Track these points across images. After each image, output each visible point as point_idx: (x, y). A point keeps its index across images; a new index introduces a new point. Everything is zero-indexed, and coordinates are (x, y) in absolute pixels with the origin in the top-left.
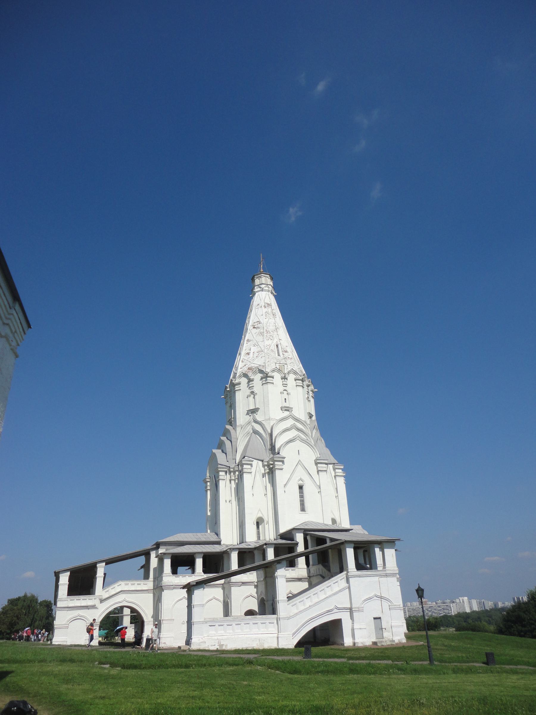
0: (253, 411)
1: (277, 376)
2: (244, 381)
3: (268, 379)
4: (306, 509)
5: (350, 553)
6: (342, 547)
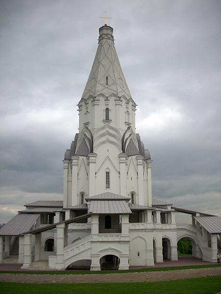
0: (87, 124)
1: (102, 99)
3: (95, 102)
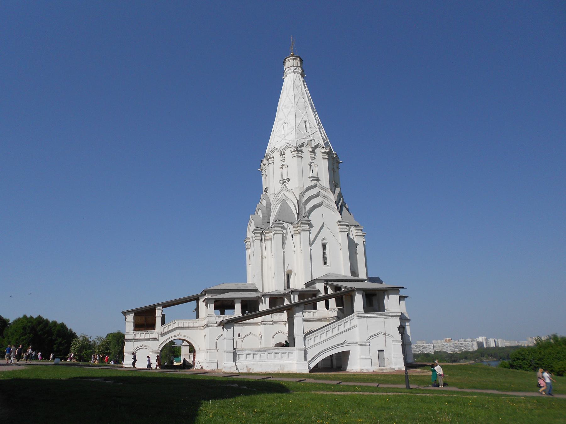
2: (277, 155)
4: (328, 263)
5: (359, 300)
6: (353, 293)
